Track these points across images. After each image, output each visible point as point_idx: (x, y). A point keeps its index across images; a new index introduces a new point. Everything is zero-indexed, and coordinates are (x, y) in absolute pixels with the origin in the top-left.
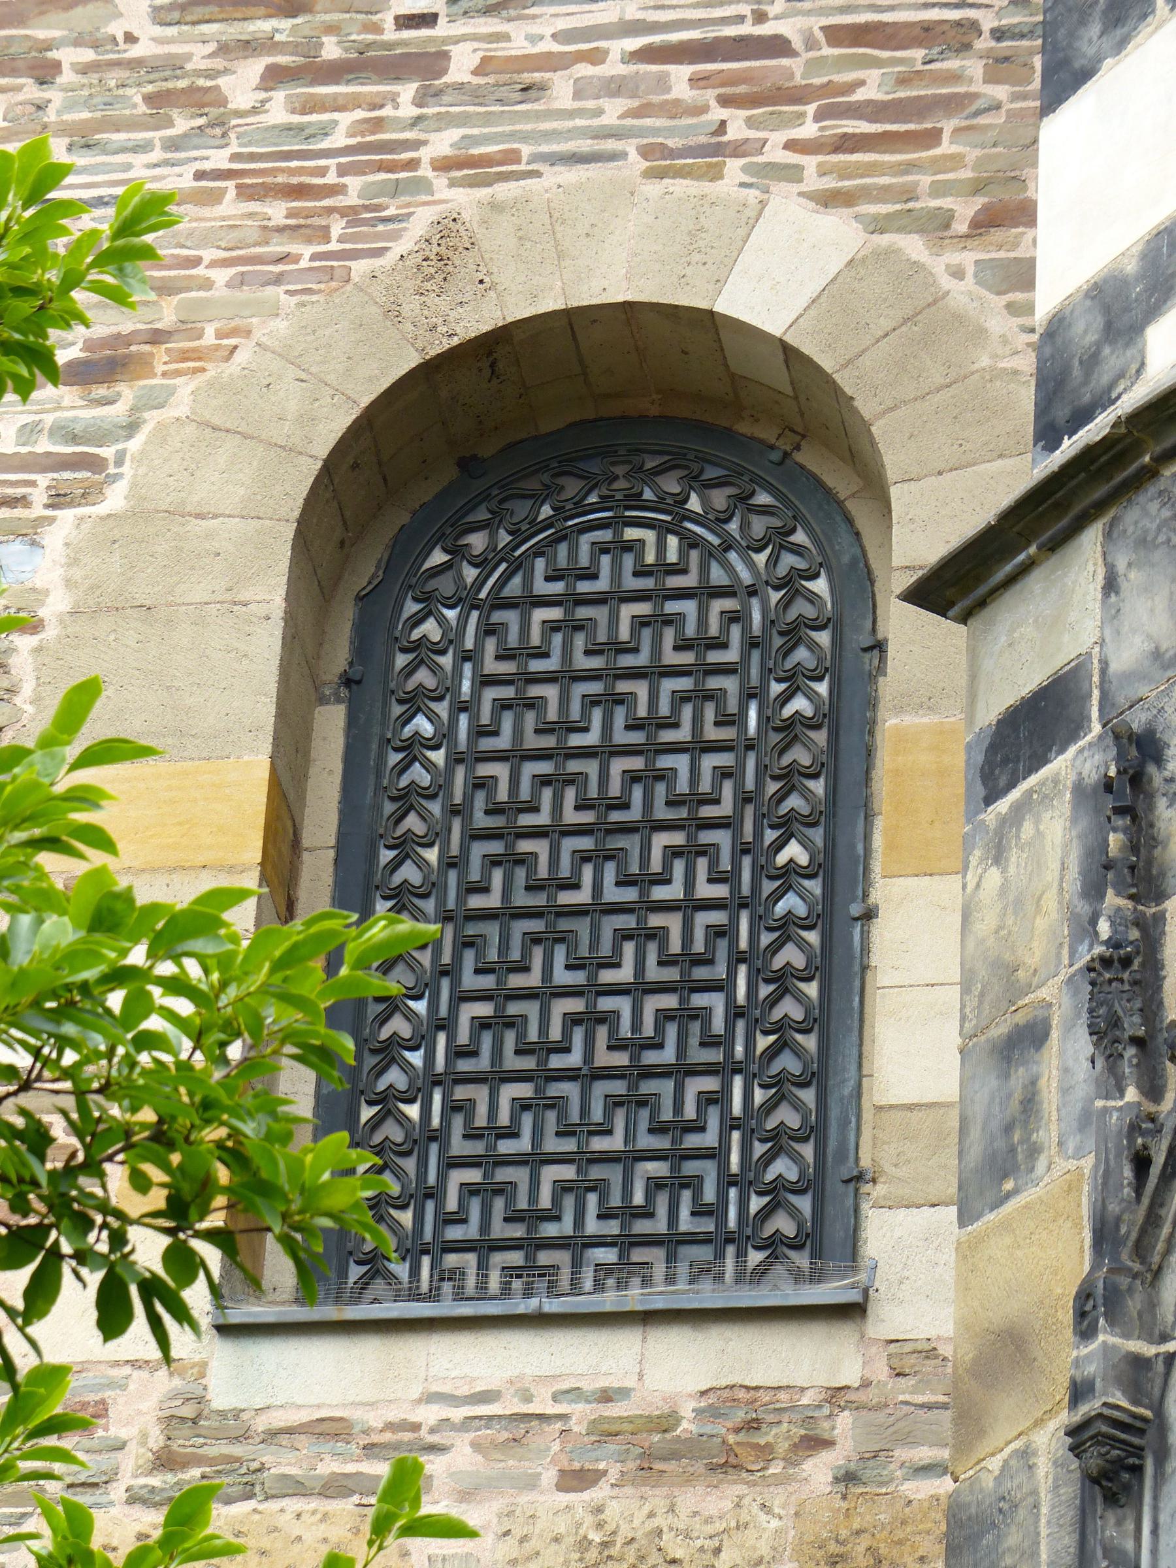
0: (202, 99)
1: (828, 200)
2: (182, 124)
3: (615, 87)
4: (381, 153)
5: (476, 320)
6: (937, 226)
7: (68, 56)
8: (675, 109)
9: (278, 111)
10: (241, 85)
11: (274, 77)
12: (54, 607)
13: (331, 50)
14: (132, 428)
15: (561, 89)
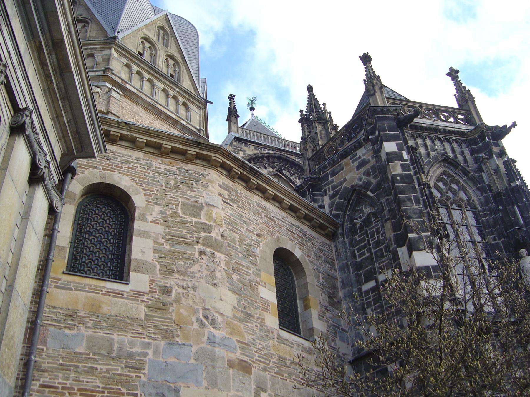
0: (261, 216)
6: (305, 255)
10: (263, 215)
12: (259, 256)
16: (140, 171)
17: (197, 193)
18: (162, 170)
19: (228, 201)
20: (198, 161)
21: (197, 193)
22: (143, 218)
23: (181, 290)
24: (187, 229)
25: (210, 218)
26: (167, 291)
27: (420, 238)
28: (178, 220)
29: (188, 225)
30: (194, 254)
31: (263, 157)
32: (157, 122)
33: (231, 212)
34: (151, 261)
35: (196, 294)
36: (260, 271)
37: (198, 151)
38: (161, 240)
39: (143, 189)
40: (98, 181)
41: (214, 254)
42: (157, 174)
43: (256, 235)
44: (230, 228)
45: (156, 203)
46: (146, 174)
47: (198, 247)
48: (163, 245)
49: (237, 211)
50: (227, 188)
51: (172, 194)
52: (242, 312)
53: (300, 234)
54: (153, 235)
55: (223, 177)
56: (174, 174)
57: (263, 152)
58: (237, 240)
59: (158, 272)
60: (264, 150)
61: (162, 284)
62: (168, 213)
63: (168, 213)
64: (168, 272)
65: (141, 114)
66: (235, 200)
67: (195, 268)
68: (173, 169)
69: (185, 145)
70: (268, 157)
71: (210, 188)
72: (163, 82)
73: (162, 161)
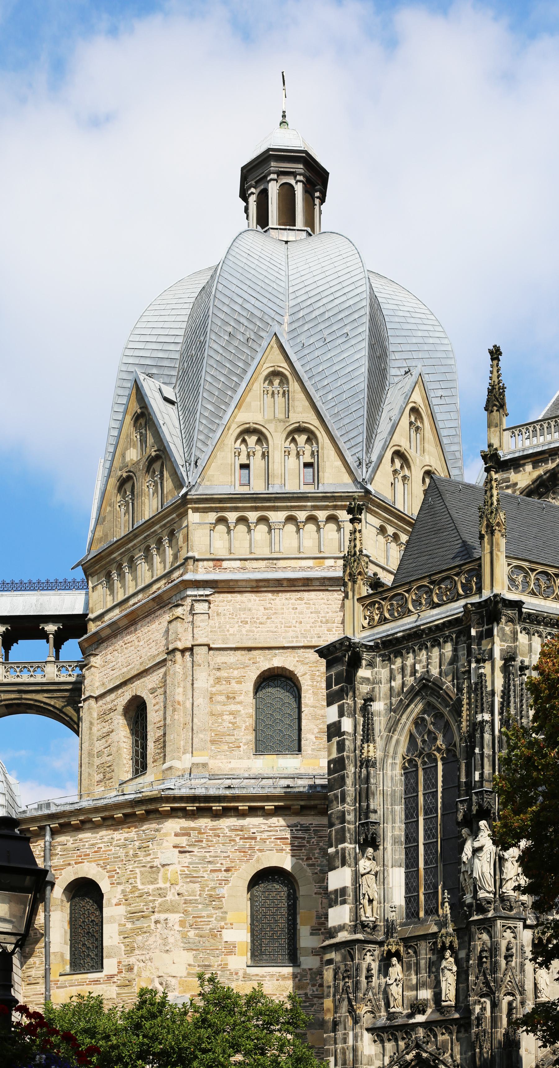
0: (234, 840)
2: (233, 843)
3: (272, 842)
4: (251, 848)
7: (221, 835)
10: (237, 839)
11: (241, 839)
15: (268, 841)
17: (152, 856)
19: (188, 849)
21: (152, 856)
23: (142, 964)
24: (144, 902)
25: (166, 880)
26: (130, 969)
28: (137, 894)
30: (149, 926)
32: (277, 601)
33: (190, 860)
34: (117, 945)
35: (152, 964)
38: (123, 921)
41: (166, 919)
43: (225, 871)
44: (188, 880)
47: (154, 917)
48: (125, 925)
49: (199, 854)
50: (185, 833)
52: (199, 966)
54: (118, 918)
58: (198, 889)
59: (123, 953)
61: (126, 963)
62: (128, 890)
63: (128, 890)
64: (130, 950)
65: (250, 605)
67: (152, 940)
71: (165, 844)
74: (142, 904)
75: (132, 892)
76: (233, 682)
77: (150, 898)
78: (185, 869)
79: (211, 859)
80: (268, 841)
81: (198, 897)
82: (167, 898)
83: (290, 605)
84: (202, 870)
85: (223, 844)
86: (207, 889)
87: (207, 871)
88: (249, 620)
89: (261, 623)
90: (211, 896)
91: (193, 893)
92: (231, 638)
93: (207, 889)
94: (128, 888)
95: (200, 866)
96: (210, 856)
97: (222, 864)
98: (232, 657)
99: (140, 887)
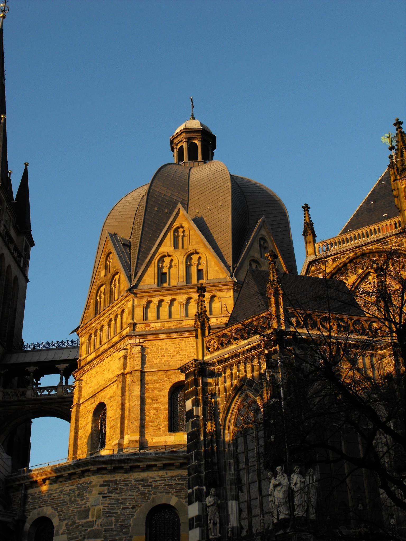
0: (138, 488)
1: (176, 496)
3: (163, 488)
5: (155, 504)
6: (182, 498)
7: (130, 484)
8: (166, 489)
9: (142, 489)
10: (140, 486)
11: (142, 486)
12: (132, 525)
13: (145, 484)
14: (135, 512)
16: (56, 499)
18: (68, 491)
20: (86, 474)
21: (85, 501)
22: (58, 534)
27: (193, 492)
29: (80, 527)
31: (345, 265)
32: (183, 343)
33: (109, 502)
36: (132, 537)
37: (81, 469)
39: (58, 512)
40: (36, 517)
42: (65, 496)
44: (107, 515)
45: (64, 520)
46: (60, 499)
49: (115, 498)
51: (72, 508)
53: (181, 481)
55: (104, 476)
56: (74, 490)
57: (343, 260)
58: (114, 521)
60: (344, 257)
62: (69, 524)
63: (69, 524)
65: (167, 346)
66: (113, 489)
68: (74, 487)
69: (74, 469)
70: (351, 261)
72: (186, 293)
73: (69, 483)
74: (78, 533)
75: (72, 525)
76: (156, 392)
77: (83, 529)
78: (106, 508)
79: (123, 501)
80: (160, 487)
81: (113, 527)
82: (94, 528)
83: (191, 345)
84: (117, 508)
85: (131, 491)
86: (119, 521)
87: (120, 509)
88: (166, 355)
89: (173, 356)
90: (122, 525)
91: (111, 524)
92: (155, 365)
93: (119, 521)
94: (70, 522)
95: (115, 505)
96: (122, 499)
97: (129, 503)
98: (155, 376)
99: (77, 521)
